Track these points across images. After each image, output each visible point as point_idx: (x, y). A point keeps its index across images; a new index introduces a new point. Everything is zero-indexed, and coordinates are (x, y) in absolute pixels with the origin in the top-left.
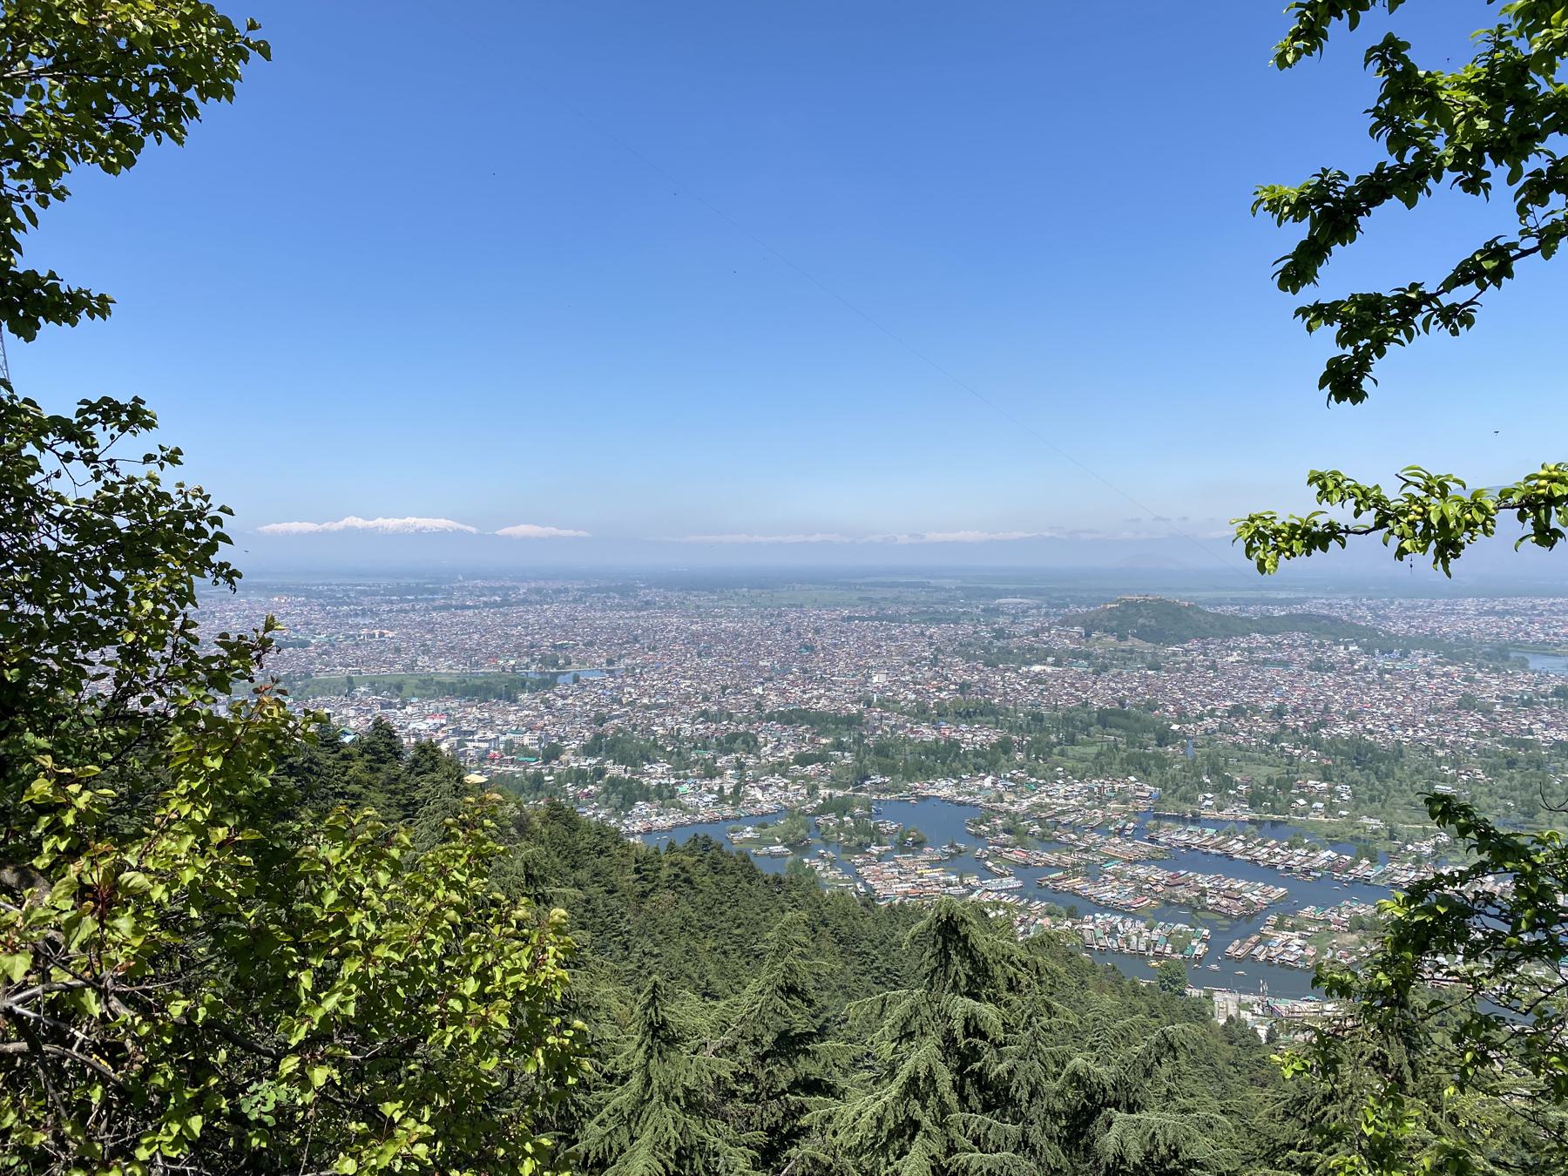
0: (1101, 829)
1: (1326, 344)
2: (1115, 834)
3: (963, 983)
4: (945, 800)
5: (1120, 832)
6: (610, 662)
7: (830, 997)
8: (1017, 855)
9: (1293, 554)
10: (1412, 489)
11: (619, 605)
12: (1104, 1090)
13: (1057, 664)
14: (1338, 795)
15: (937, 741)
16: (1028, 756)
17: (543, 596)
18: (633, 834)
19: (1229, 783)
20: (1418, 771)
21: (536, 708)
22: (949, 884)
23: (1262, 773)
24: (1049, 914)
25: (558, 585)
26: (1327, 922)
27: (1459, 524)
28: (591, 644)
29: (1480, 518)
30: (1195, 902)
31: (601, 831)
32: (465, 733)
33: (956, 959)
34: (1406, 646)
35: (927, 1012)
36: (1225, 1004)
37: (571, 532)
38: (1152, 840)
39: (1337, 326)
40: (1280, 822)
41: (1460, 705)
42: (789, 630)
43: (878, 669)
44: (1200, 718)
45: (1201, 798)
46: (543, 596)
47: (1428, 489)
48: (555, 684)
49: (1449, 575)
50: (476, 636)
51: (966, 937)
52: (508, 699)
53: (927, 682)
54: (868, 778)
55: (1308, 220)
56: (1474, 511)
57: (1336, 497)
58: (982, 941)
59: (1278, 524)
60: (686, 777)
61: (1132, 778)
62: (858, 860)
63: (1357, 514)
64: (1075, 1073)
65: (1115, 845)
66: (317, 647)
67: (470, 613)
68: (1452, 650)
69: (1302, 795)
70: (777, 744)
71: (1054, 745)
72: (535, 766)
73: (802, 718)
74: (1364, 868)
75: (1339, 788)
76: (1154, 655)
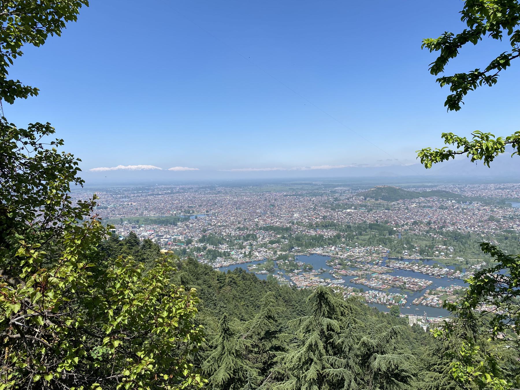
0: (371, 263)
1: (447, 91)
2: (375, 265)
3: (326, 313)
4: (319, 255)
5: (377, 264)
6: (207, 212)
7: (282, 320)
8: (343, 272)
9: (437, 162)
10: (476, 138)
11: (209, 193)
12: (373, 347)
13: (355, 209)
15: (316, 235)
16: (346, 239)
17: (184, 190)
18: (216, 268)
19: (413, 247)
21: (183, 227)
22: (321, 282)
23: (424, 243)
24: (354, 291)
25: (189, 186)
26: (446, 292)
27: (492, 149)
28: (200, 206)
29: (499, 147)
30: (402, 286)
31: (206, 267)
32: (160, 236)
33: (324, 306)
34: (471, 200)
35: (314, 323)
36: (413, 320)
37: (193, 169)
38: (387, 266)
39: (451, 84)
41: (489, 220)
42: (266, 200)
43: (296, 212)
44: (403, 225)
45: (403, 252)
46: (184, 190)
47: (482, 138)
48: (189, 219)
49: (489, 167)
50: (163, 204)
51: (327, 298)
52: (174, 224)
53: (312, 216)
54: (293, 248)
55: (440, 50)
56: (498, 144)
57: (451, 141)
58: (332, 300)
59: (432, 152)
60: (233, 249)
61: (381, 246)
62: (291, 275)
63: (458, 147)
64: (364, 342)
65: (375, 268)
66: (110, 209)
67: (160, 196)
68: (486, 202)
69: (437, 250)
70: (263, 238)
71: (355, 236)
72: (183, 246)
73: (271, 229)
74: (458, 274)
75: (449, 248)
76: (387, 205)
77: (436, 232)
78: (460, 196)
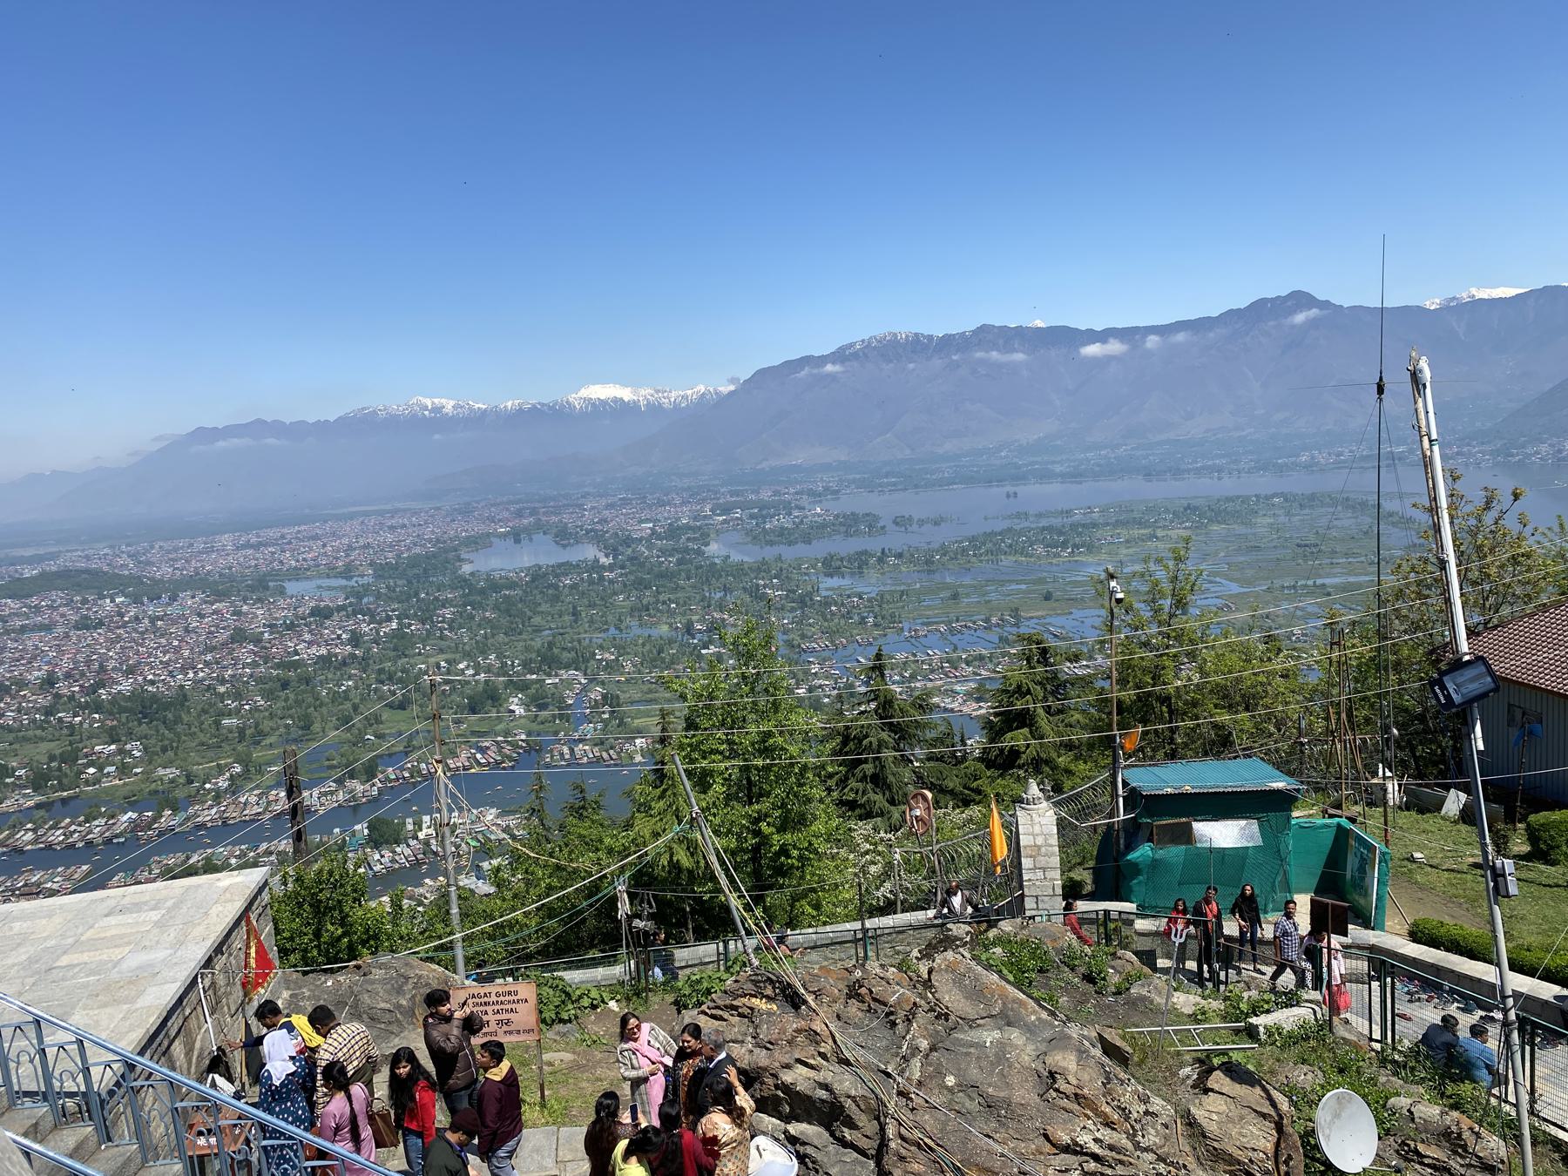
14: (129, 754)
20: (204, 711)
34: (174, 589)
40: (70, 798)
41: (233, 639)
68: (220, 587)
74: (167, 819)
75: (128, 747)
77: (80, 706)
78: (137, 580)
